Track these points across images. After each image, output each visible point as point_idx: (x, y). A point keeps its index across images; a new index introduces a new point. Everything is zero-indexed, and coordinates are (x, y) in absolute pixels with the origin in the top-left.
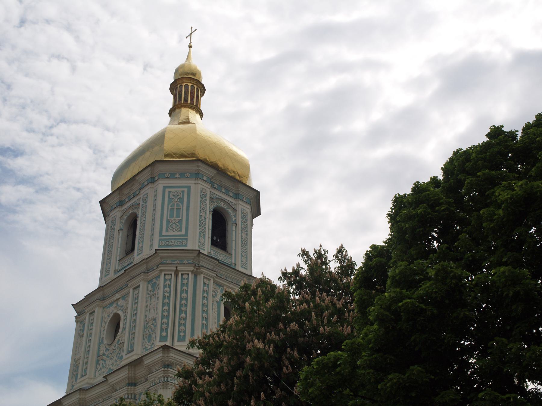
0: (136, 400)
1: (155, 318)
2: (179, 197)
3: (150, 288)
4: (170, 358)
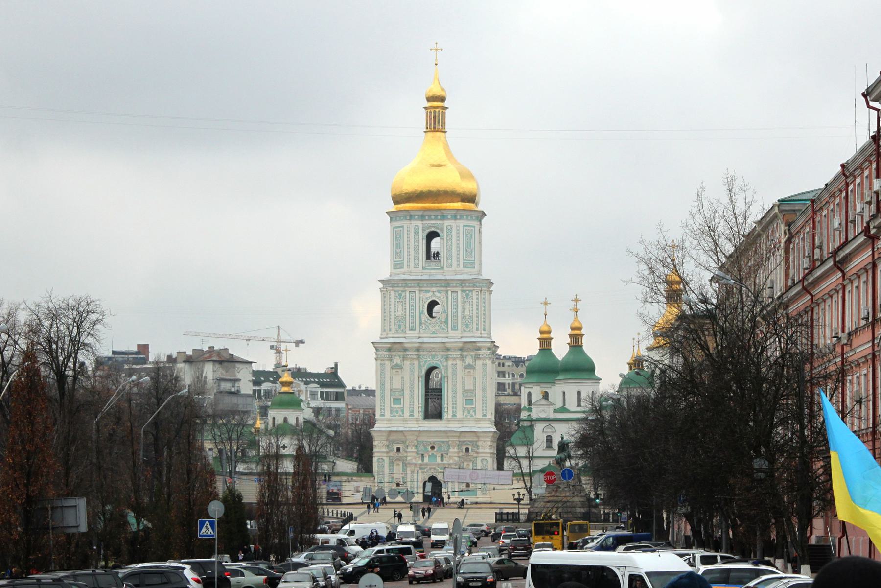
3: (464, 296)
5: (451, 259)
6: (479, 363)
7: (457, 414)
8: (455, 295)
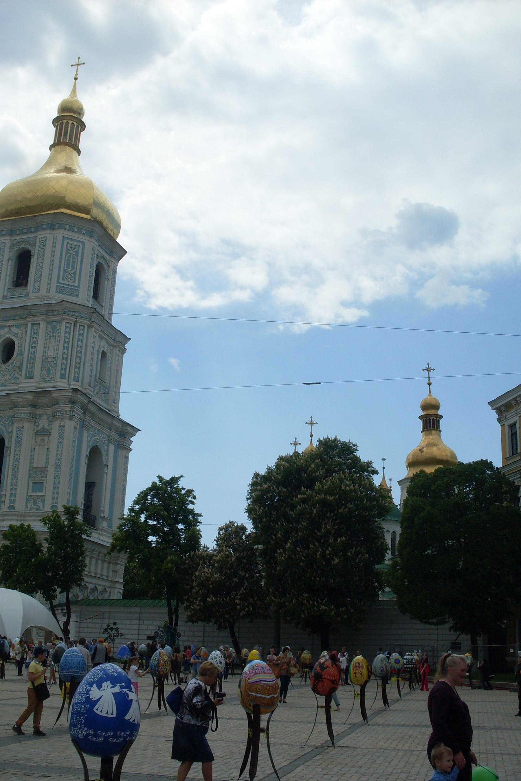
0: (36, 419)
1: (55, 356)
2: (75, 250)
3: (49, 329)
4: (77, 398)
5: (40, 282)
6: (56, 424)
7: (16, 506)
8: (36, 328)
